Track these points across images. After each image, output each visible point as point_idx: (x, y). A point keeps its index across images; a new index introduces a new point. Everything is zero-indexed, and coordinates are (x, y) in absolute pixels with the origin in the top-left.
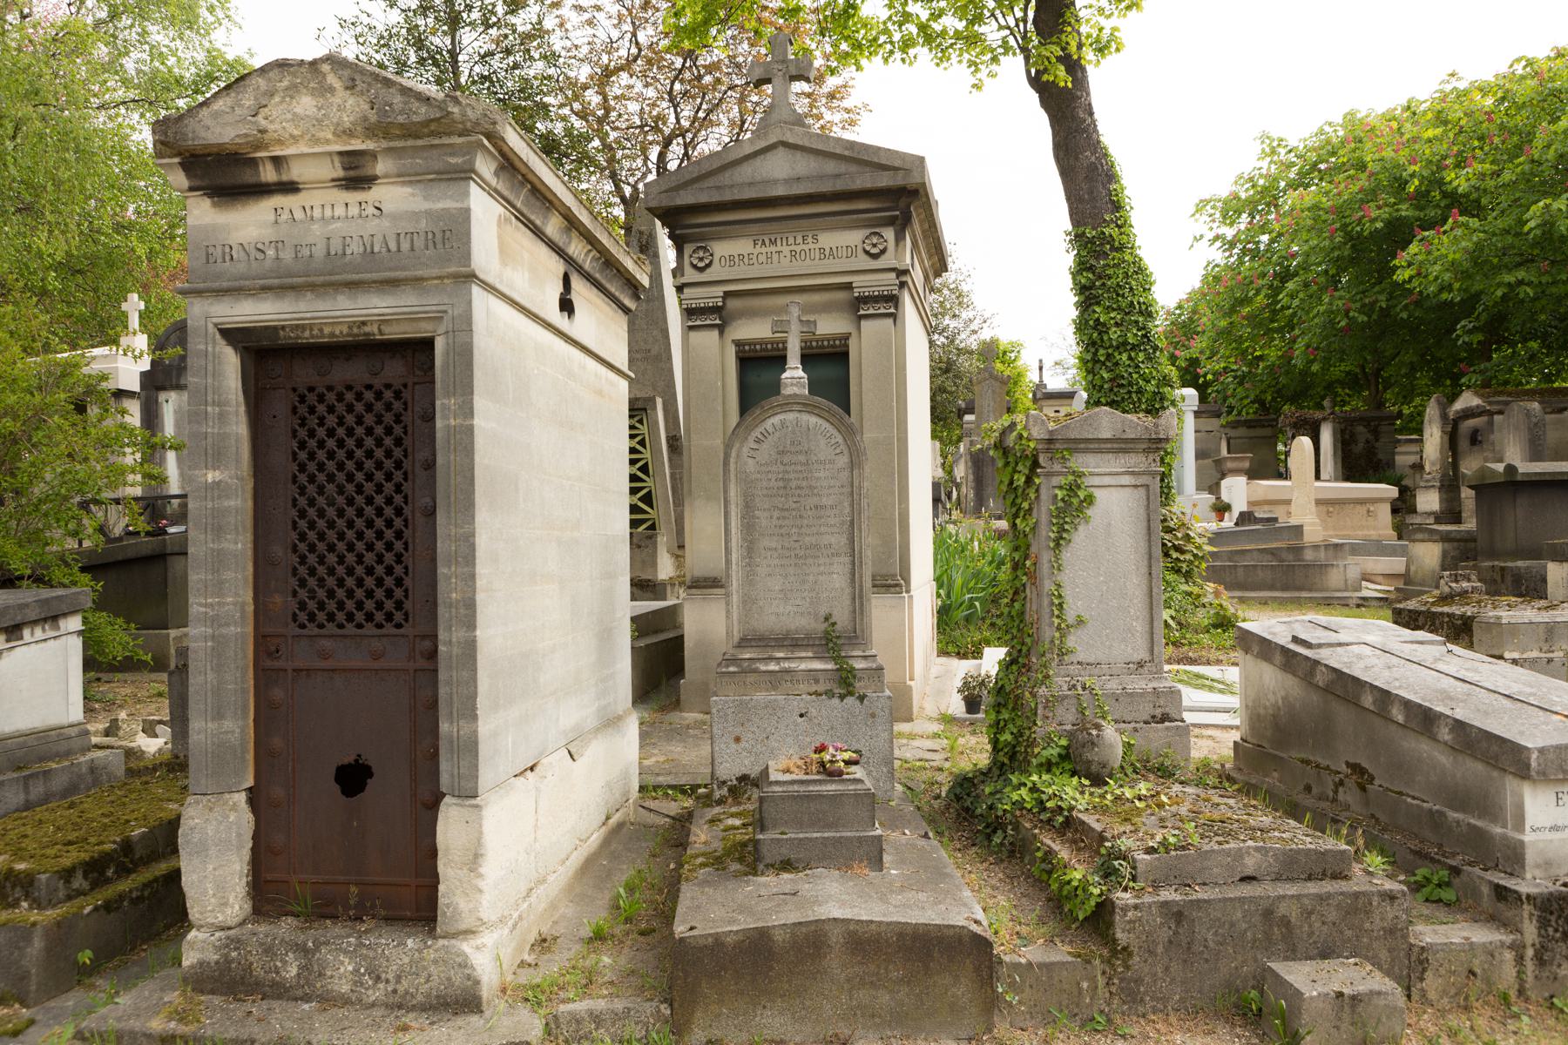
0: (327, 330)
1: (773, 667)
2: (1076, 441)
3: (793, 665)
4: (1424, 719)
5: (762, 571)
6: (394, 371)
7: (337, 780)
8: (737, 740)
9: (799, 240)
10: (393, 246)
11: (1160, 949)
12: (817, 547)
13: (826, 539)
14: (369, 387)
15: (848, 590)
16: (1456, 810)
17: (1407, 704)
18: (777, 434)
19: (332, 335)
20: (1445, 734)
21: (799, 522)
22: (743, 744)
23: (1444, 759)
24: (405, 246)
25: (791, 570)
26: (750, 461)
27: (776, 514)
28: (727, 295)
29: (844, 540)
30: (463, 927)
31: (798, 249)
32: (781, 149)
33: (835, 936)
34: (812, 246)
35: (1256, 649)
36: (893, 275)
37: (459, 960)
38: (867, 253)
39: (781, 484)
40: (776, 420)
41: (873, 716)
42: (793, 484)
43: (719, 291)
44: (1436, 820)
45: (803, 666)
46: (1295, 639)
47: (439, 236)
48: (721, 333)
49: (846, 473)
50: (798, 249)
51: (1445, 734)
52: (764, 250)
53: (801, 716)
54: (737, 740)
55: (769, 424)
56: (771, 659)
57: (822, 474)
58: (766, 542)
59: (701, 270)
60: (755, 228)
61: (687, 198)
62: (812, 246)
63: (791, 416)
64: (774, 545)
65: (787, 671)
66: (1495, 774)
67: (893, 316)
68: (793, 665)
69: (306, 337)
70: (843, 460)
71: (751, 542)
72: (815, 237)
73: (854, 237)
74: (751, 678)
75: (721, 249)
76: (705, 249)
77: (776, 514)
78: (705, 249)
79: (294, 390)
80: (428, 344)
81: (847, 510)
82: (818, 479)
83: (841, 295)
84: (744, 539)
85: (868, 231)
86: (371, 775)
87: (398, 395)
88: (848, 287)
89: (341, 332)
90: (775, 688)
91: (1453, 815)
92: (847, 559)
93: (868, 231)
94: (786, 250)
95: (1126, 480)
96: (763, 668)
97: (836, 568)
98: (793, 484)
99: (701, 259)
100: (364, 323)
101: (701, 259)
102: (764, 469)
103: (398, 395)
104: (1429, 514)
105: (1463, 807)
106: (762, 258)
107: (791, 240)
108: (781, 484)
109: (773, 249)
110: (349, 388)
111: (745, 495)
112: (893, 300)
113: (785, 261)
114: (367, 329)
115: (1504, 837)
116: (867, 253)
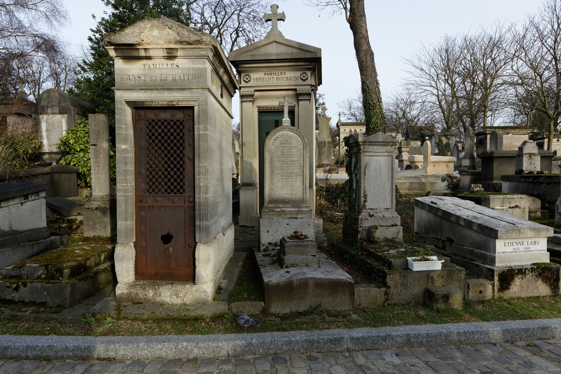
0: (160, 103)
1: (278, 210)
2: (372, 142)
3: (285, 209)
4: (469, 224)
5: (275, 180)
6: (179, 115)
7: (162, 239)
8: (268, 232)
9: (280, 74)
10: (182, 78)
11: (399, 286)
12: (292, 173)
13: (295, 171)
14: (172, 121)
15: (302, 187)
16: (477, 249)
17: (465, 220)
19: (162, 104)
20: (475, 228)
21: (287, 165)
23: (475, 235)
24: (186, 78)
25: (284, 180)
27: (280, 163)
28: (256, 91)
29: (301, 171)
30: (204, 281)
31: (279, 77)
32: (274, 43)
33: (311, 283)
34: (284, 76)
35: (420, 205)
36: (310, 87)
37: (203, 290)
40: (280, 133)
41: (309, 224)
43: (253, 89)
44: (472, 252)
45: (288, 210)
46: (432, 202)
47: (197, 75)
48: (253, 104)
49: (302, 150)
50: (279, 77)
51: (475, 228)
52: (268, 77)
54: (268, 232)
55: (278, 134)
56: (278, 207)
57: (294, 151)
58: (277, 171)
59: (247, 82)
60: (265, 69)
61: (242, 58)
62: (284, 76)
63: (285, 132)
65: (283, 211)
66: (489, 238)
67: (309, 100)
68: (285, 209)
69: (154, 105)
70: (301, 146)
72: (285, 73)
73: (298, 74)
74: (272, 213)
75: (253, 76)
77: (280, 163)
78: (248, 75)
79: (148, 121)
80: (192, 108)
81: (302, 162)
85: (302, 72)
86: (172, 238)
87: (181, 124)
89: (164, 104)
91: (476, 250)
92: (302, 177)
93: (302, 72)
94: (275, 77)
95: (386, 154)
97: (298, 180)
98: (286, 153)
99: (247, 79)
100: (172, 101)
101: (247, 79)
103: (181, 124)
104: (466, 167)
105: (479, 247)
106: (267, 79)
107: (277, 74)
109: (271, 76)
110: (165, 121)
112: (309, 94)
113: (275, 81)
114: (173, 103)
115: (491, 255)
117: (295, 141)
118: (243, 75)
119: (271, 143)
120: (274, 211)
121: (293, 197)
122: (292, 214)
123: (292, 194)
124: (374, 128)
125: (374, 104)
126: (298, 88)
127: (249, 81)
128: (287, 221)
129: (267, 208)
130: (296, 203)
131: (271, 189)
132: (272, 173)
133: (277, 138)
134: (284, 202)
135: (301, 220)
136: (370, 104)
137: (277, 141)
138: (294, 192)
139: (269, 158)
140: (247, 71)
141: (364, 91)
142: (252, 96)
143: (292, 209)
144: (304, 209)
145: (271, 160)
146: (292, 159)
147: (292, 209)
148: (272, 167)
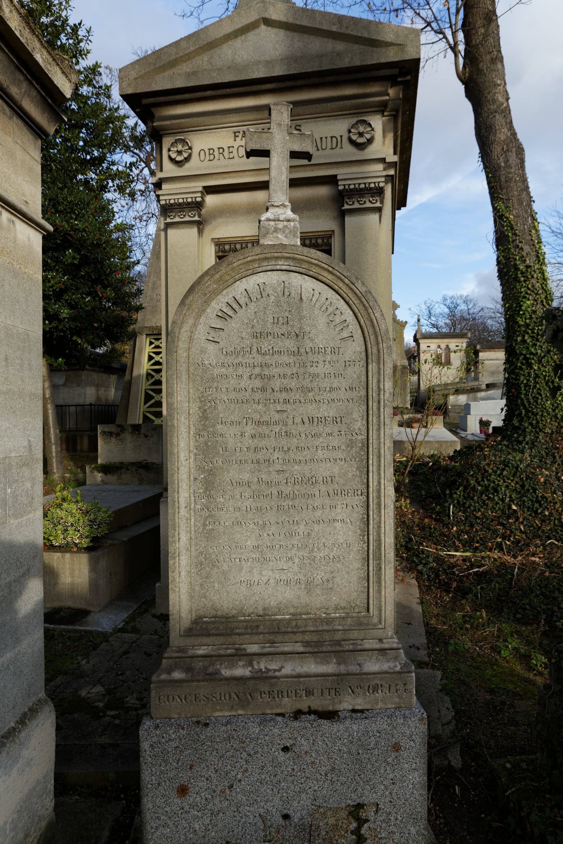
1: (241, 671)
8: (183, 791)
12: (311, 481)
13: (323, 470)
15: (357, 547)
18: (252, 307)
21: (283, 442)
22: (192, 798)
25: (271, 517)
26: (211, 347)
27: (249, 430)
32: (263, 27)
36: (380, 167)
38: (351, 141)
39: (258, 383)
40: (251, 283)
41: (397, 748)
42: (277, 384)
43: (199, 185)
45: (288, 669)
48: (200, 232)
49: (359, 368)
53: (286, 749)
55: (240, 288)
56: (240, 655)
57: (321, 369)
58: (233, 473)
59: (179, 164)
60: (235, 118)
61: (162, 83)
63: (272, 279)
64: (246, 477)
65: (262, 677)
67: (379, 210)
70: (357, 346)
71: (211, 472)
73: (339, 127)
75: (200, 142)
76: (184, 142)
77: (249, 430)
78: (184, 142)
81: (359, 424)
82: (315, 376)
83: (323, 191)
84: (200, 469)
88: (332, 180)
90: (243, 704)
92: (359, 500)
93: (354, 120)
96: (226, 673)
97: (340, 513)
98: (277, 384)
99: (179, 153)
101: (179, 153)
102: (230, 360)
108: (258, 383)
111: (202, 400)
116: (351, 141)
117: (322, 320)
118: (167, 142)
119: (202, 331)
120: (213, 677)
121: (318, 602)
122: (309, 693)
123: (309, 586)
124: (527, 325)
125: (528, 267)
126: (341, 172)
127: (187, 159)
128: (282, 732)
129: (185, 662)
130: (327, 638)
131: (204, 564)
132: (209, 482)
133: (235, 306)
134: (270, 628)
135: (356, 727)
136: (517, 269)
137: (233, 324)
138: (320, 576)
139: (195, 408)
140: (182, 130)
141: (501, 240)
142: (198, 206)
143: (312, 667)
144: (373, 666)
145: (204, 416)
146: (311, 409)
147: (312, 667)
148: (207, 450)
